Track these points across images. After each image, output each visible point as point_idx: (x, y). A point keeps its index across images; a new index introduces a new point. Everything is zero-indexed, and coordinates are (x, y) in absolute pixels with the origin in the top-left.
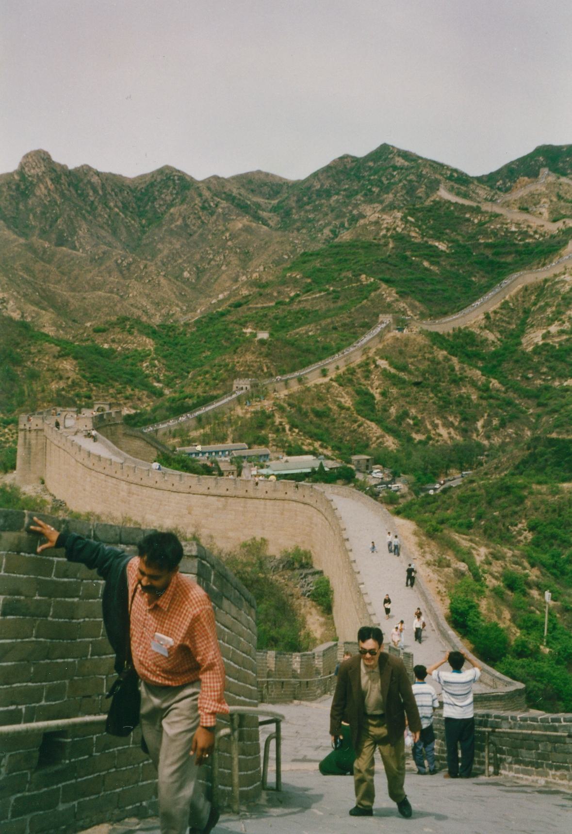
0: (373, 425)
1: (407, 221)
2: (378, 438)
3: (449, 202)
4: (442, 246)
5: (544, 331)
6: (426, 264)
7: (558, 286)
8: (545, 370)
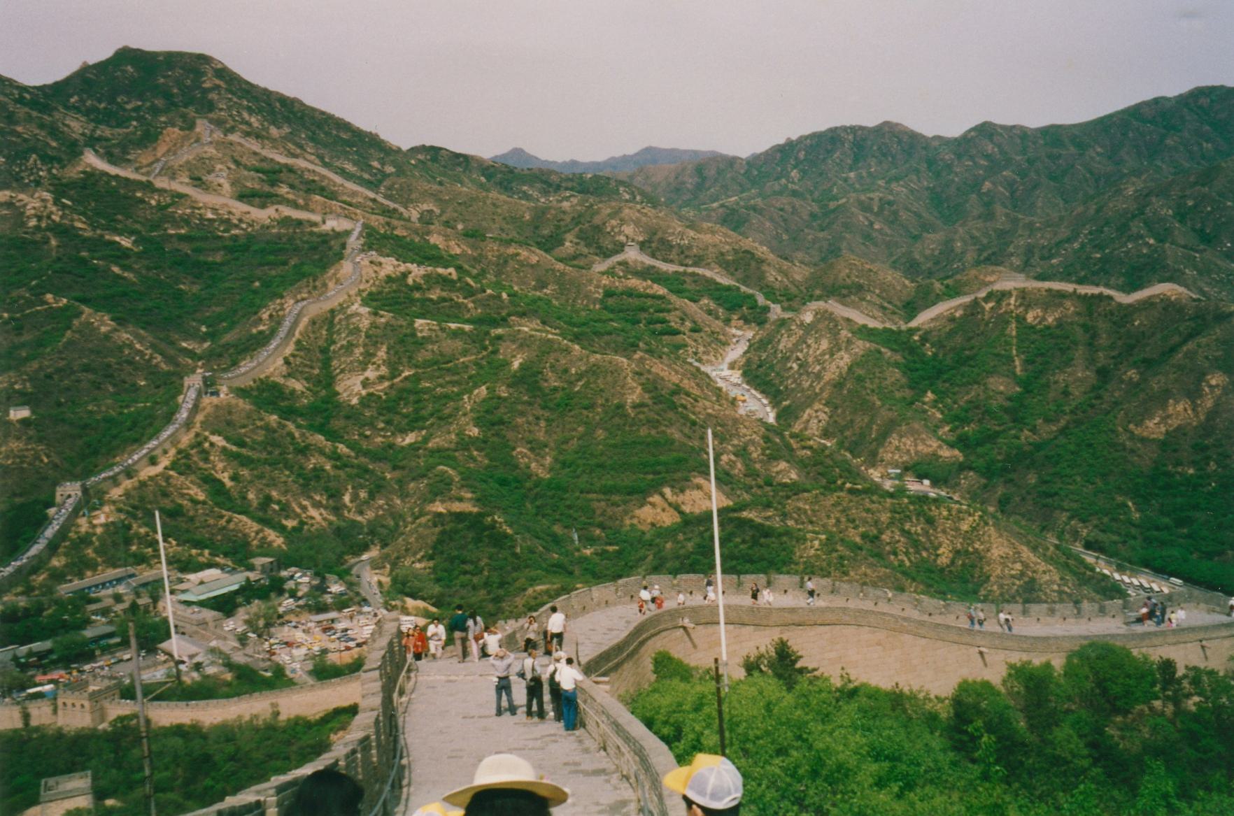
0: (244, 518)
1: (64, 206)
2: (257, 533)
3: (107, 174)
4: (126, 242)
5: (362, 378)
6: (116, 269)
7: (354, 320)
8: (381, 425)
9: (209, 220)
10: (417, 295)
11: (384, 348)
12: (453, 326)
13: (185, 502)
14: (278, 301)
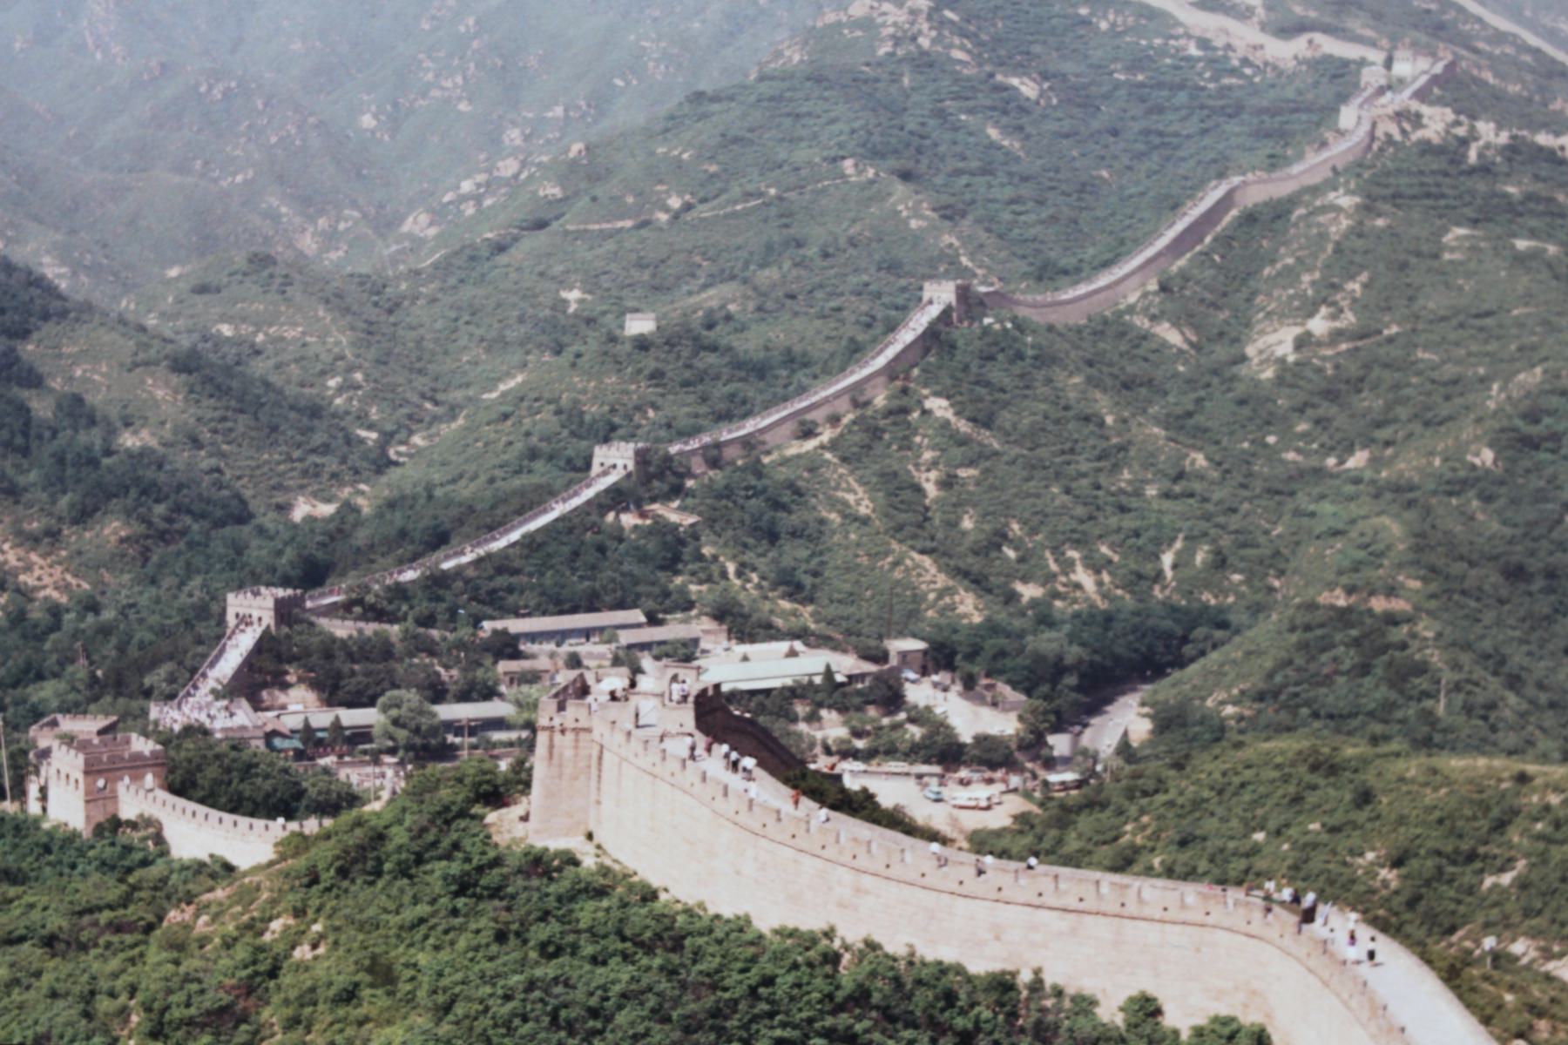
0: (927, 561)
1: (943, 22)
2: (940, 596)
4: (1028, 88)
5: (1298, 330)
6: (993, 133)
7: (1321, 219)
8: (1302, 427)
9: (1189, 59)
10: (1481, 186)
11: (1364, 277)
12: (1522, 244)
13: (833, 516)
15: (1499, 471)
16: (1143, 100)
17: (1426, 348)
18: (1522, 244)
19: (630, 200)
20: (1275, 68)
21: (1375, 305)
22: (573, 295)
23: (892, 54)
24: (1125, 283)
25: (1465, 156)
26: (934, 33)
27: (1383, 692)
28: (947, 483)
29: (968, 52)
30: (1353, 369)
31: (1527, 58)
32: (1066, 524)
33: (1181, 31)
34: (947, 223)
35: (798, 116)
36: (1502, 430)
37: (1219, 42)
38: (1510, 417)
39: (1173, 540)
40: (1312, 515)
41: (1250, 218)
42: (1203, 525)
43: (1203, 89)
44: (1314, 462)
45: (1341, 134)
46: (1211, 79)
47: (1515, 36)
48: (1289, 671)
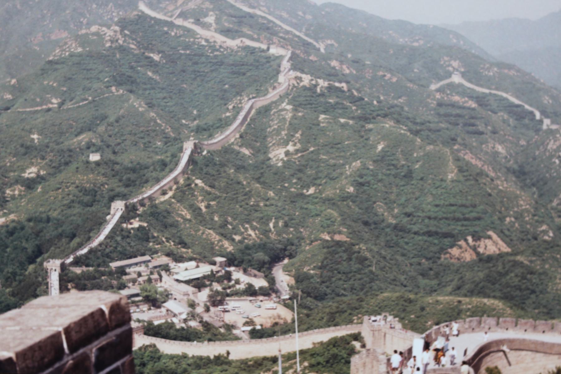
0: (211, 232)
1: (125, 35)
2: (218, 243)
3: (149, 16)
4: (156, 57)
5: (284, 150)
6: (150, 74)
7: (283, 113)
8: (294, 181)
9: (203, 46)
10: (322, 99)
11: (300, 132)
12: (342, 120)
13: (179, 219)
14: (239, 98)
15: (355, 193)
16: (191, 60)
17: (323, 155)
18: (342, 120)
19: (38, 100)
20: (230, 49)
21: (306, 140)
22: (35, 136)
23: (111, 47)
24: (228, 135)
25: (316, 90)
26: (123, 39)
27: (357, 266)
28: (207, 207)
29: (135, 45)
30: (304, 163)
31: (296, 39)
32: (243, 217)
33: (199, 36)
34: (151, 109)
35: (88, 70)
36: (354, 181)
37: (212, 40)
38: (354, 177)
39: (271, 219)
40: (306, 209)
41: (259, 112)
42: (280, 214)
43: (209, 56)
44: (300, 191)
45: (279, 84)
46: (211, 53)
47: (292, 32)
48: (328, 260)
